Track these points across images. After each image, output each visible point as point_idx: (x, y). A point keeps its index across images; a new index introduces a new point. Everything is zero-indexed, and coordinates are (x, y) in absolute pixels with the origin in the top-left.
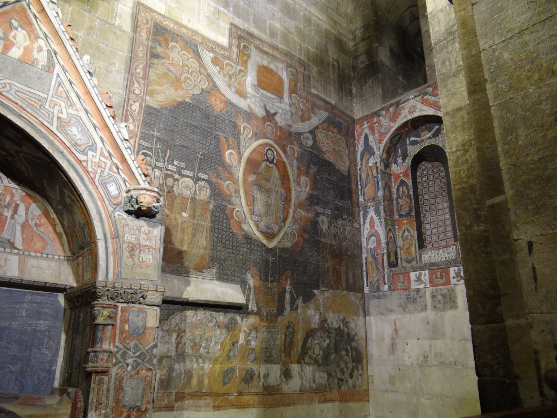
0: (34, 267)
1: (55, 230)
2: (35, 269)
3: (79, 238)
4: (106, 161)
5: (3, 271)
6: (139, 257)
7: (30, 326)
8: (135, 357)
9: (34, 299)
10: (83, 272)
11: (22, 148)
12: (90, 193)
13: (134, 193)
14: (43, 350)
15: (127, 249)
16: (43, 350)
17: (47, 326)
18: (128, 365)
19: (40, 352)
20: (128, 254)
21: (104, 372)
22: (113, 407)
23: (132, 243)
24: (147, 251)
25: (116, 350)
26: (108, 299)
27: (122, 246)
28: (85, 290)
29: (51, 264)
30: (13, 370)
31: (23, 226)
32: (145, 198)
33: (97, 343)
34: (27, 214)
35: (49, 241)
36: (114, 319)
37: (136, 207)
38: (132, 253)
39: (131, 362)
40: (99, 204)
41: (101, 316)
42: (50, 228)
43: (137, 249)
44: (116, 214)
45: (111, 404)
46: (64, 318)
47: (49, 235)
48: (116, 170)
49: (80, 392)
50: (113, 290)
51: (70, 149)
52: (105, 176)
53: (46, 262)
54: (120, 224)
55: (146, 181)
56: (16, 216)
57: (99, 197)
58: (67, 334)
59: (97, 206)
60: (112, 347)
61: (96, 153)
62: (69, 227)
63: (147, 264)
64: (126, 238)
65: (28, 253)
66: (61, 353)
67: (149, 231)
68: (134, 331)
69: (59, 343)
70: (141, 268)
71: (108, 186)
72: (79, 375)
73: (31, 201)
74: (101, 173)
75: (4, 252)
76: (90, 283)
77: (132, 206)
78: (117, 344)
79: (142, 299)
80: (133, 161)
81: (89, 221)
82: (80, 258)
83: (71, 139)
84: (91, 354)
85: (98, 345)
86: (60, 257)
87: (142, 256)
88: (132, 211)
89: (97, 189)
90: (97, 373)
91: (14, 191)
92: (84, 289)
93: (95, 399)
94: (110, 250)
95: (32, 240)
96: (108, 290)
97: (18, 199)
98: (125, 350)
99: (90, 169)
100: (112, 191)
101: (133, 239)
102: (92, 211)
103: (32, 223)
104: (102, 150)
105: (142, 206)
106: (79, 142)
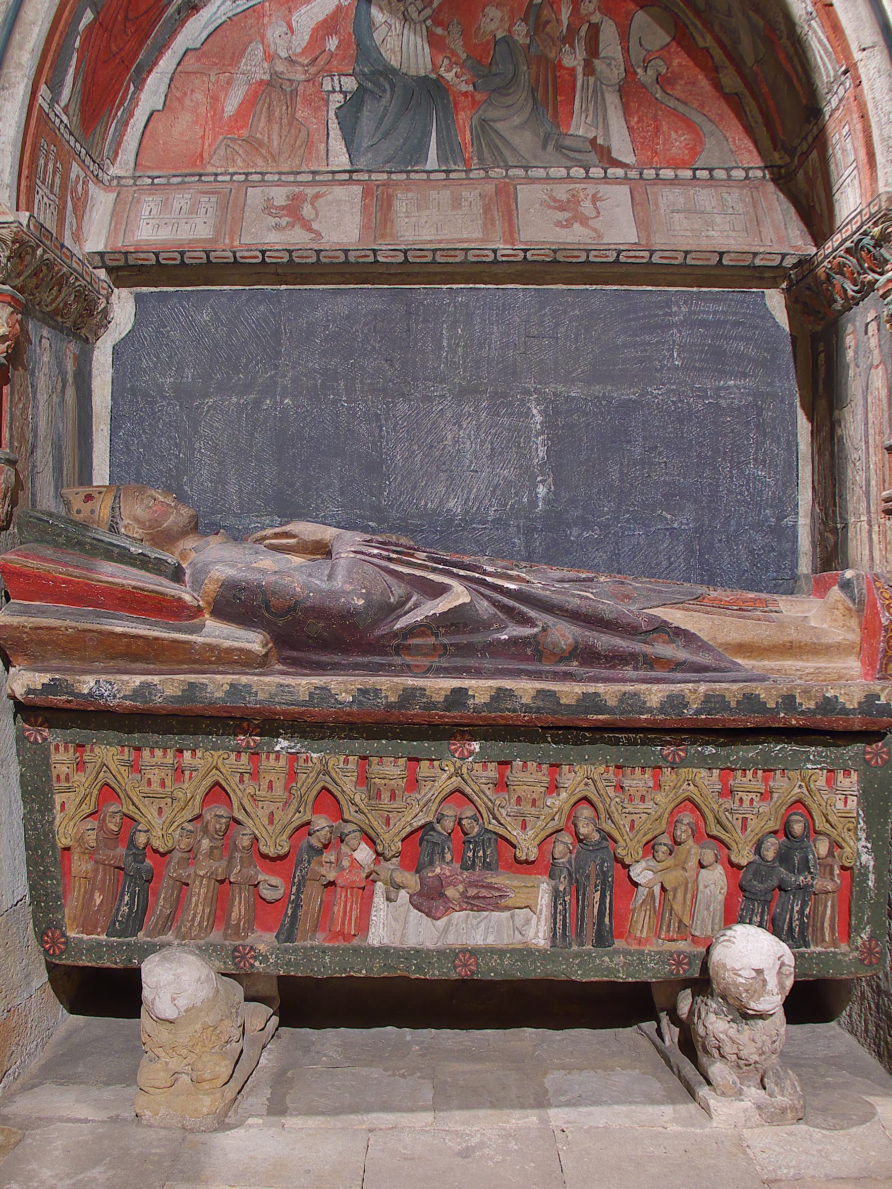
1: (717, 86)
2: (682, 215)
5: (595, 230)
9: (695, 313)
17: (748, 395)
29: (725, 195)
30: (675, 526)
34: (626, 50)
56: (596, 62)
58: (811, 419)
62: (758, 61)
65: (653, 171)
69: (792, 446)
72: (870, 532)
75: (588, 177)
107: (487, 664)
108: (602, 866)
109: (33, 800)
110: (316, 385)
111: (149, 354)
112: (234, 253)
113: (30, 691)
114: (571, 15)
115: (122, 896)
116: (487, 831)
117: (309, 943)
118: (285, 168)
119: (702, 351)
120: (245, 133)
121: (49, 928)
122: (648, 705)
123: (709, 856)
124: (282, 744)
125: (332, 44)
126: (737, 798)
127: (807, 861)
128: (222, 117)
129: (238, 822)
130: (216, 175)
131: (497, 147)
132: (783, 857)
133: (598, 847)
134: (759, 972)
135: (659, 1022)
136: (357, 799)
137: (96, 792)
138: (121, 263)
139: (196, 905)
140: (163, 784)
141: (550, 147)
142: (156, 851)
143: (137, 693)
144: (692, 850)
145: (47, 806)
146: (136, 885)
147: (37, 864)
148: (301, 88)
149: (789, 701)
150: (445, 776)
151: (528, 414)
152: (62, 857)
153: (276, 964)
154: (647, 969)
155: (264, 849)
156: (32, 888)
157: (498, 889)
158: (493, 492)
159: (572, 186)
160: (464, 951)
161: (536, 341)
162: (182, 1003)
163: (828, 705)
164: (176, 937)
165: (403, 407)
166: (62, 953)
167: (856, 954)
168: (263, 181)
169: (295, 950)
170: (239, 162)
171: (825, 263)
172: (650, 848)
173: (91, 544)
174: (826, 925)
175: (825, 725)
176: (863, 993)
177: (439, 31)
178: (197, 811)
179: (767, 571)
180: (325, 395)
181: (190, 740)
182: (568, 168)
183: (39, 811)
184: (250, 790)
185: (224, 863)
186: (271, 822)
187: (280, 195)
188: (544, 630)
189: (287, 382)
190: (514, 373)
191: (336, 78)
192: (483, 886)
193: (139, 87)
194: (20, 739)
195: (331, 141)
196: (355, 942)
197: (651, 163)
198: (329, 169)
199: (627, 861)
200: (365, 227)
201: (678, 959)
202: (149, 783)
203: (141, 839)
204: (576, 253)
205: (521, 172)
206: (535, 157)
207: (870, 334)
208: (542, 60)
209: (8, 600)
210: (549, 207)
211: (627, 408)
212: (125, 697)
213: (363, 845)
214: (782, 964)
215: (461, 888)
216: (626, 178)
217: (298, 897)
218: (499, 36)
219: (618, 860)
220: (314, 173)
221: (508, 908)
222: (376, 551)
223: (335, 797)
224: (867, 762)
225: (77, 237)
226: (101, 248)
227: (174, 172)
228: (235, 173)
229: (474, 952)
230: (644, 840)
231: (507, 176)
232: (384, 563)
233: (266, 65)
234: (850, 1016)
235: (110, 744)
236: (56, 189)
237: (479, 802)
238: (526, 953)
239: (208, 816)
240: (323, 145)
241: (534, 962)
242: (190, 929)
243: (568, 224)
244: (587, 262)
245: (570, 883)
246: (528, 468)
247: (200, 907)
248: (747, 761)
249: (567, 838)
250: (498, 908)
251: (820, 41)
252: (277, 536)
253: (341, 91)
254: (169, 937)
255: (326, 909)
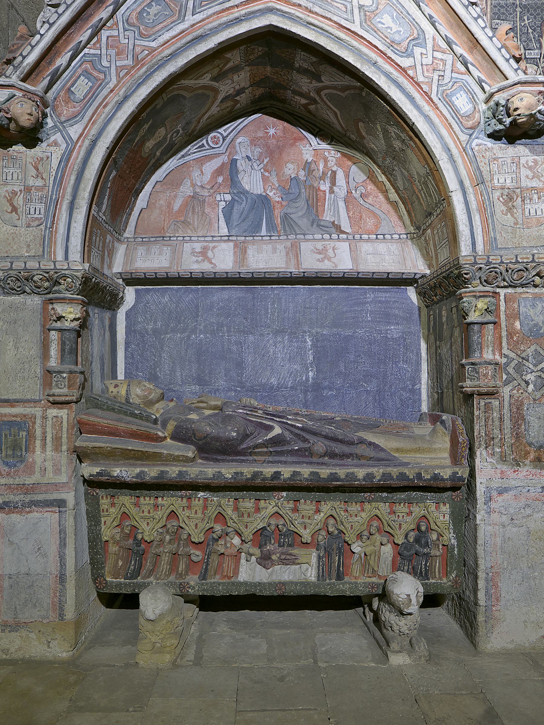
0: (370, 254)
1: (387, 198)
2: (371, 256)
3: (422, 202)
4: (444, 57)
5: (334, 263)
6: (523, 210)
7: (379, 333)
8: (537, 371)
10: (436, 251)
11: (322, 82)
12: (427, 118)
13: (500, 98)
14: (401, 364)
15: (501, 199)
16: (401, 364)
18: (527, 383)
19: (397, 366)
20: (504, 208)
21: (491, 394)
22: (512, 445)
23: (509, 188)
24: (536, 196)
25: (504, 360)
26: (481, 283)
27: (491, 196)
28: (444, 274)
30: (368, 389)
31: (346, 201)
32: (521, 99)
33: (475, 351)
34: (348, 183)
35: (383, 216)
36: (495, 314)
37: (508, 121)
38: (510, 204)
39: (533, 378)
40: (444, 132)
41: (475, 311)
42: (381, 197)
43: (517, 197)
44: (474, 144)
45: (509, 440)
46: (420, 320)
47: (380, 207)
48: (463, 69)
49: (459, 421)
50: (488, 267)
51: (385, 54)
52: (446, 84)
53: (384, 244)
54: (482, 159)
55: (519, 69)
57: (442, 122)
59: (441, 138)
60: (497, 357)
61: (426, 48)
62: (405, 189)
63: (538, 220)
64: (496, 181)
65: (359, 236)
66: (424, 367)
67: (536, 162)
68: (531, 330)
69: (419, 354)
70: (528, 228)
71: (454, 98)
72: (453, 397)
73: (350, 163)
74: (439, 80)
75: (331, 239)
76: (450, 263)
77: (500, 122)
78: (505, 351)
79: (537, 277)
80: (491, 38)
81: (432, 165)
82: (429, 231)
83: (384, 39)
84: (467, 367)
85: (477, 354)
86: (401, 236)
87: (529, 206)
88: (500, 130)
89: (437, 108)
90: (480, 394)
91: (326, 154)
92: (441, 274)
93: (484, 432)
94: (474, 205)
95: (361, 217)
96: (480, 268)
97: (333, 164)
98: (521, 360)
99: (421, 79)
100: (462, 106)
101: (508, 181)
102: (435, 147)
103: (356, 194)
104: (434, 39)
105: (519, 115)
106: (397, 38)
107: (289, 459)
108: (339, 545)
109: (92, 521)
110: (214, 329)
111: (141, 316)
112: (178, 273)
113: (91, 475)
114: (324, 167)
115: (131, 561)
116: (289, 530)
117: (212, 581)
118: (200, 234)
119: (380, 314)
120: (182, 219)
121: (98, 577)
122: (358, 477)
123: (385, 540)
124: (201, 494)
125: (220, 179)
126: (397, 515)
127: (428, 542)
128: (172, 212)
129: (182, 528)
130: (170, 237)
131: (292, 225)
132: (417, 540)
133: (337, 537)
134: (408, 596)
135: (364, 609)
136: (233, 517)
137: (119, 516)
138: (129, 277)
139: (164, 565)
140: (149, 512)
141: (315, 225)
142: (146, 541)
143: (138, 475)
144: (378, 538)
145: (98, 523)
146: (137, 557)
147: (93, 549)
148: (207, 199)
149: (419, 476)
150: (271, 507)
151: (305, 342)
152: (105, 545)
153: (198, 590)
154: (359, 590)
155: (193, 540)
156: (91, 559)
157: (294, 556)
158: (290, 375)
159: (324, 243)
160: (280, 583)
161: (308, 310)
162: (158, 612)
163: (436, 477)
164: (155, 579)
165: (251, 338)
166: (104, 587)
167: (450, 583)
168: (191, 240)
169: (207, 584)
170: (180, 232)
171: (434, 280)
172: (360, 536)
173: (118, 409)
174: (437, 570)
175: (435, 485)
176: (453, 597)
177: (267, 174)
178: (164, 524)
179: (408, 408)
180: (218, 333)
181: (161, 493)
182: (322, 235)
183: (95, 525)
184: (188, 515)
185: (176, 545)
186: (196, 527)
187: (198, 247)
188: (313, 444)
189: (202, 327)
190: (299, 324)
191: (222, 195)
192: (287, 554)
193: (136, 199)
194: (86, 494)
195: (220, 222)
196: (232, 580)
197: (358, 232)
198: (219, 235)
199: (350, 542)
200: (235, 262)
201: (373, 585)
202: (143, 512)
203: (140, 537)
204: (326, 273)
205: (302, 237)
206: (308, 230)
207: (453, 312)
208: (312, 187)
209: (81, 433)
210: (314, 253)
211: (347, 339)
212: (133, 477)
213: (236, 537)
214: (418, 592)
215: (278, 555)
216: (347, 238)
217: (208, 561)
218: (292, 176)
219: (347, 542)
220: (212, 236)
221: (299, 564)
222: (241, 411)
223: (224, 516)
224: (453, 500)
225: (110, 267)
226: (120, 271)
227: (152, 236)
228: (179, 237)
229: (284, 584)
230: (357, 534)
231: (296, 238)
232: (245, 416)
233: (191, 189)
234: (448, 606)
235: (126, 495)
236: (100, 249)
237: (286, 518)
238: (306, 584)
239: (169, 526)
240: (217, 224)
241: (310, 587)
242: (161, 575)
243: (322, 260)
244: (331, 277)
245: (325, 552)
246: (305, 365)
247: (165, 566)
248: (401, 499)
249: (324, 533)
250: (294, 564)
251: (432, 185)
252: (198, 402)
253: (224, 201)
254: (152, 579)
255: (220, 565)
